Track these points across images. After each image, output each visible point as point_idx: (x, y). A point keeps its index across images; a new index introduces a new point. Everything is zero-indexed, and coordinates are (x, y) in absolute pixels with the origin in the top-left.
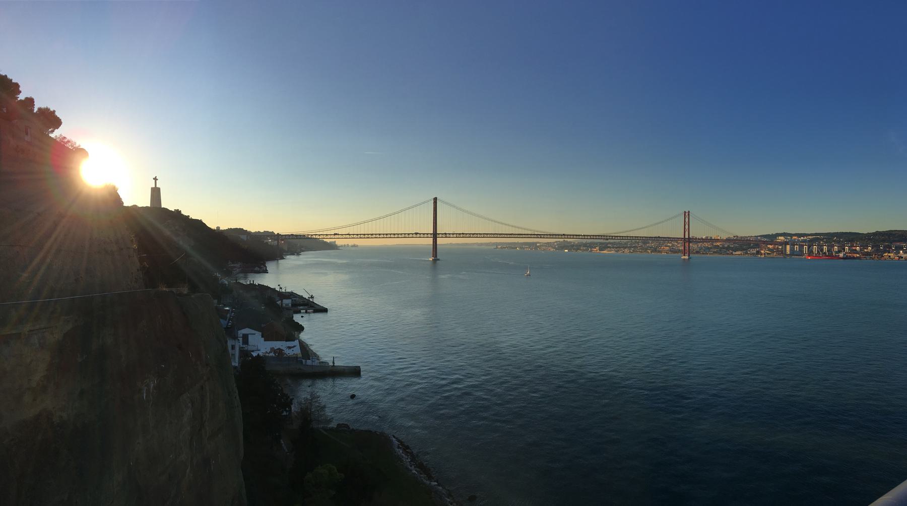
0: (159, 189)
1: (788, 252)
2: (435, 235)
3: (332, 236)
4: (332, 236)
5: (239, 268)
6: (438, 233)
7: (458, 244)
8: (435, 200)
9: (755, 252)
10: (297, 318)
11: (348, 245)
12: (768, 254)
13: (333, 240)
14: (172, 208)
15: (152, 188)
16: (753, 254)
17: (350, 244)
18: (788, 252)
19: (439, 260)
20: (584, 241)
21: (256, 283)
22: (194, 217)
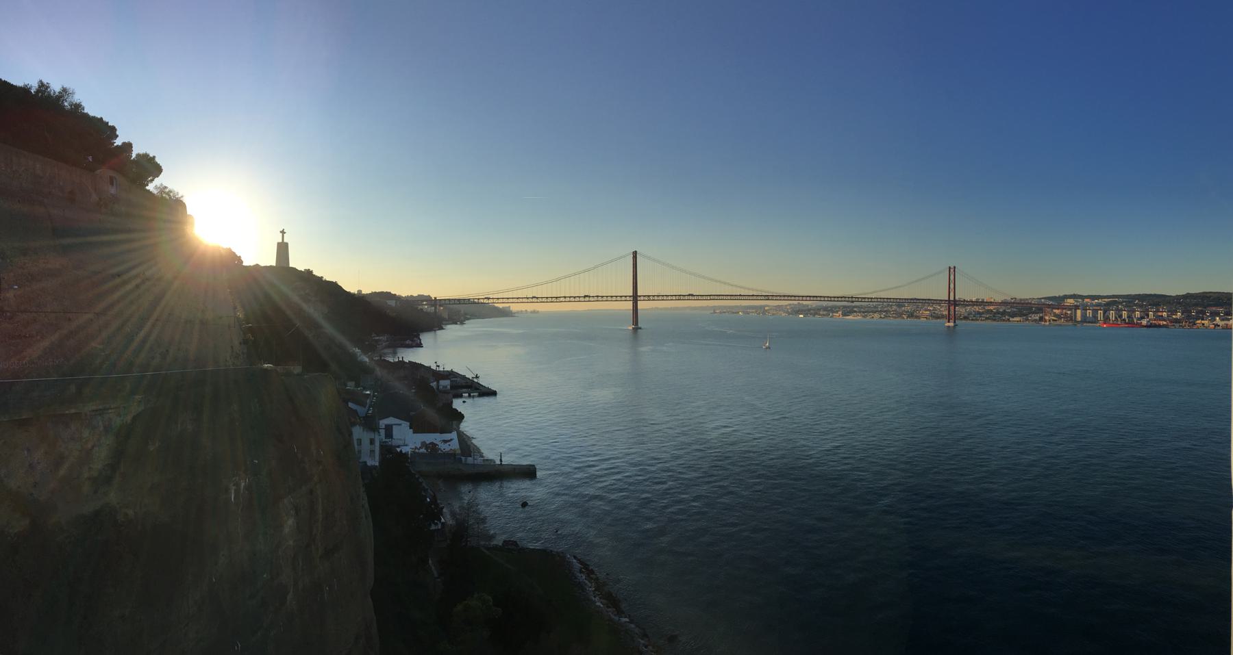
0: (287, 244)
1: (1079, 318)
2: (635, 298)
3: (505, 300)
4: (505, 300)
5: (387, 341)
6: (638, 294)
7: (666, 309)
8: (635, 254)
9: (1037, 318)
10: (458, 404)
11: (526, 311)
12: (1054, 320)
13: (507, 305)
14: (301, 268)
15: (278, 243)
16: (1035, 320)
17: (529, 310)
18: (1079, 318)
19: (640, 328)
20: (825, 304)
21: (406, 360)
22: (328, 279)
